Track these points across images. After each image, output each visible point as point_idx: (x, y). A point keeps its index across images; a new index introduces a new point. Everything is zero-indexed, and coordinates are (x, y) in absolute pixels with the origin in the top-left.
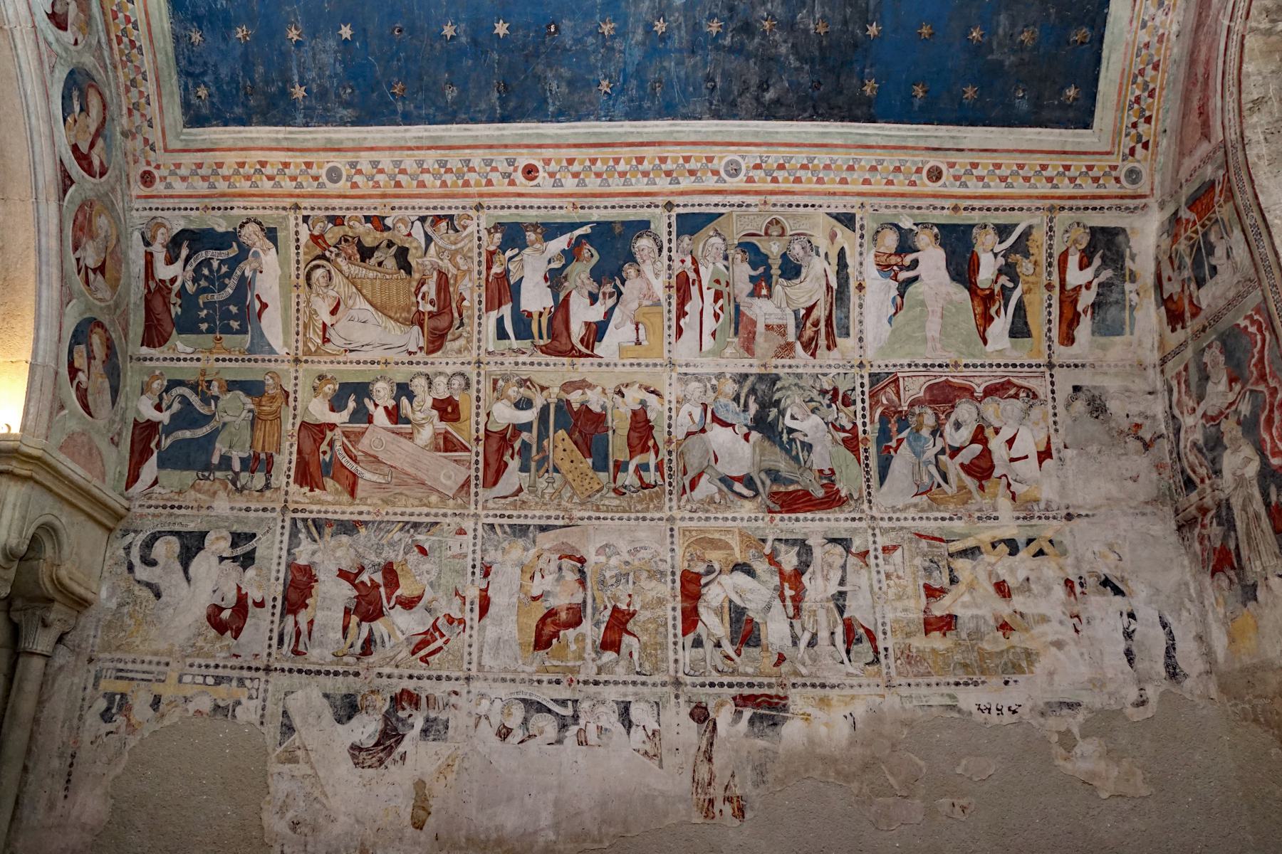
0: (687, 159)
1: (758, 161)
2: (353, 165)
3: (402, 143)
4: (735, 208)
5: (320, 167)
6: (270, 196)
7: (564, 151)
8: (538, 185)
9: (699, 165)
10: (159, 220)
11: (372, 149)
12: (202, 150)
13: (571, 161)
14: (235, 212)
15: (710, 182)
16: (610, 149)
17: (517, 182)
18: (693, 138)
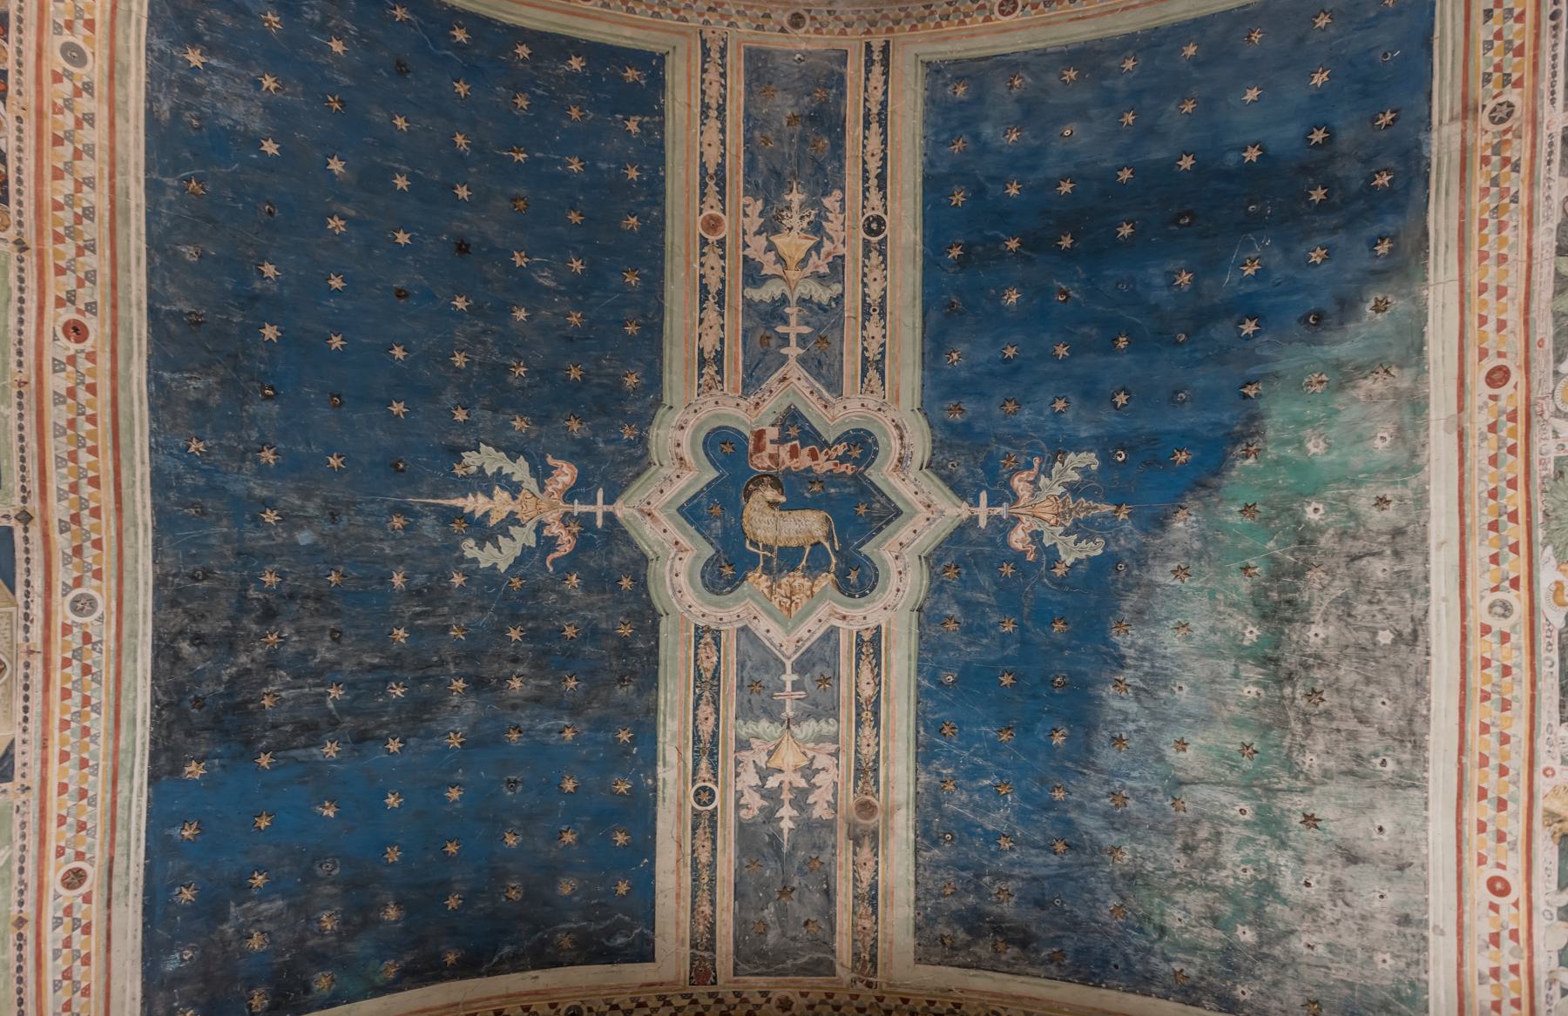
0: (97, 544)
1: (95, 639)
2: (88, 87)
3: (119, 168)
4: (22, 610)
5: (86, 39)
7: (108, 382)
8: (55, 338)
9: (90, 560)
11: (112, 124)
13: (92, 389)
15: (62, 576)
16: (109, 444)
17: (61, 310)
18: (127, 552)
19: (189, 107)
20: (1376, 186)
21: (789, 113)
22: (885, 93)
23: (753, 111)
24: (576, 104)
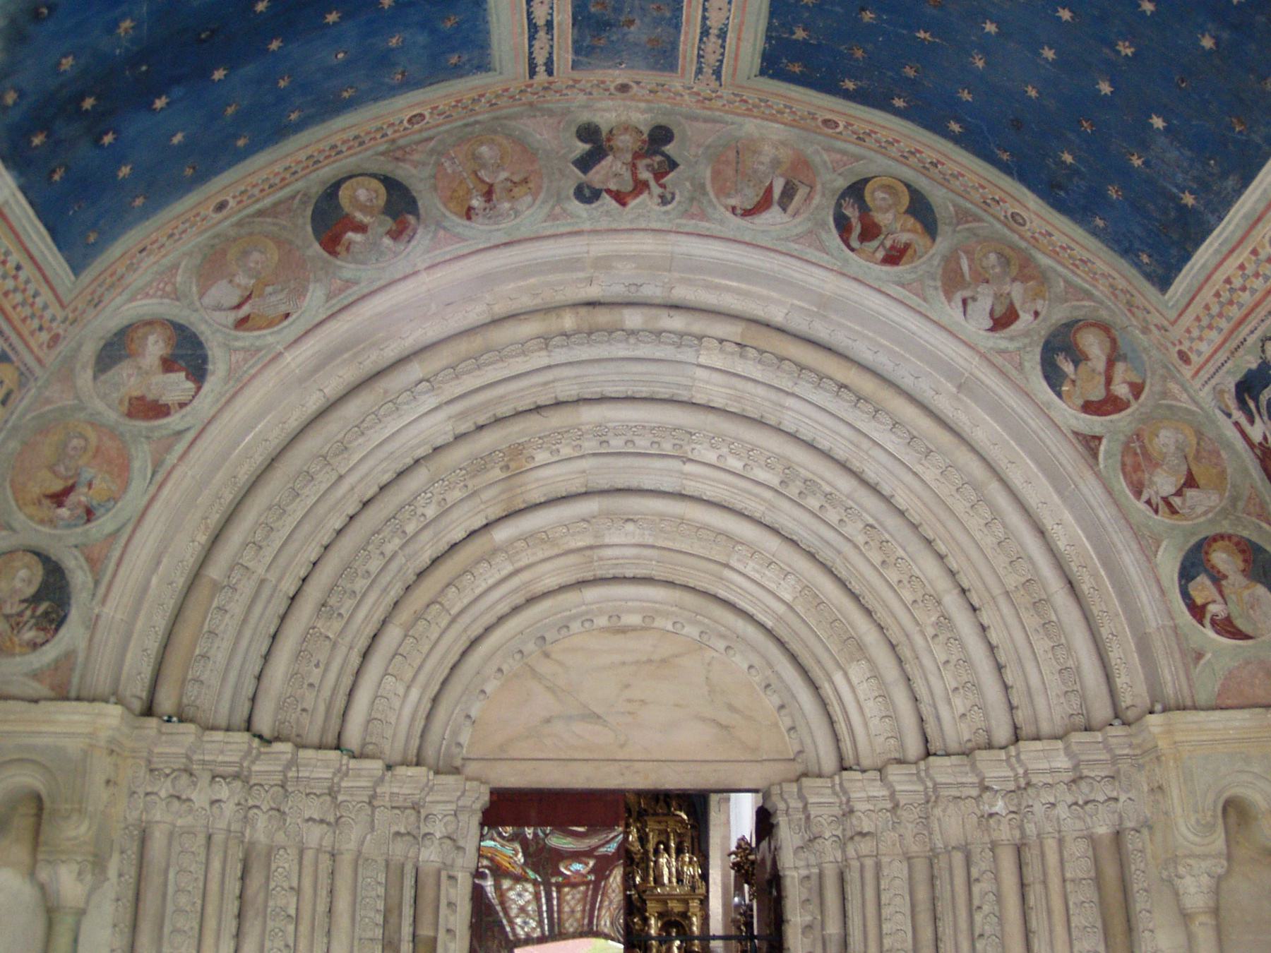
5: (1263, 247)
6: (1257, 305)
10: (1219, 388)
12: (1188, 305)
14: (1250, 340)
19: (1211, 175)
20: (42, 132)
21: (632, 28)
22: (531, 46)
23: (672, 30)
24: (857, 59)
